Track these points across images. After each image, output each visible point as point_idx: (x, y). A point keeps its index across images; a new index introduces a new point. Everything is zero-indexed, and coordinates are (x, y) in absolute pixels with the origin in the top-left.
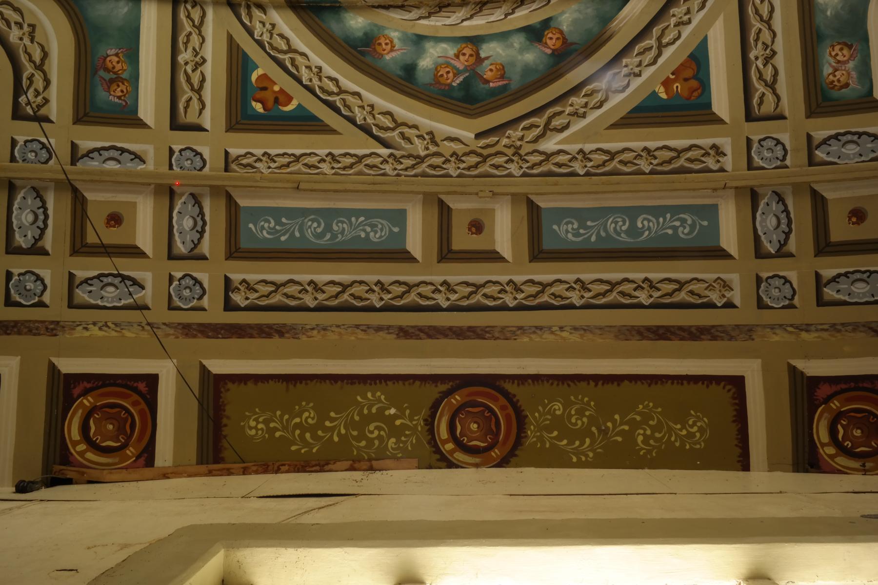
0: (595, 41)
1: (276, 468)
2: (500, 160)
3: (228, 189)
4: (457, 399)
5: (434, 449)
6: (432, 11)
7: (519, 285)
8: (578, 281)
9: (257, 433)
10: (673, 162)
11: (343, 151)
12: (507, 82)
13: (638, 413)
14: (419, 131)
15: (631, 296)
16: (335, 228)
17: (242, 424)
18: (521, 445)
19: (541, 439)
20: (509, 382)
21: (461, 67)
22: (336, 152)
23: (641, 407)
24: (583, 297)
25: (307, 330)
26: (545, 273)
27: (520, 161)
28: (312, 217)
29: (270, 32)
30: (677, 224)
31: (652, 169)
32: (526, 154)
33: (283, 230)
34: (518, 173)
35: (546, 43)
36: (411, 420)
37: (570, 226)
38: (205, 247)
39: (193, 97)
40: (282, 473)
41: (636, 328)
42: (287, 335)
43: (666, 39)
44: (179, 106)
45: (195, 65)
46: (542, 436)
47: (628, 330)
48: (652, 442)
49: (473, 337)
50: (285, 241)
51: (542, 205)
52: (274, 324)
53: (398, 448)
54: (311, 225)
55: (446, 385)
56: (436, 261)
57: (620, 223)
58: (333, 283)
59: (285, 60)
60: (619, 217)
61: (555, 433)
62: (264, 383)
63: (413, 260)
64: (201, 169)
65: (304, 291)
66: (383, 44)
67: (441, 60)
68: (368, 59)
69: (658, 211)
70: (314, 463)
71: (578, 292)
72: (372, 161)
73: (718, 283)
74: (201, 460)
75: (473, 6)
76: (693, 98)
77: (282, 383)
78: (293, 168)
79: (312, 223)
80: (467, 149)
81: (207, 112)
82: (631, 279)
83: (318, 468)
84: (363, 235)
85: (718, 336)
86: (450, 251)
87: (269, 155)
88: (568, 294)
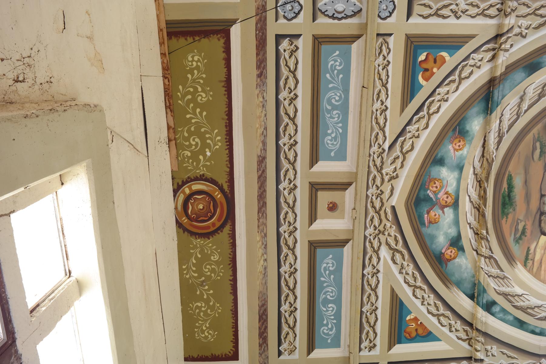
0: (446, 278)
1: (166, 76)
2: (376, 222)
3: (364, 36)
4: (218, 195)
5: (185, 181)
6: (478, 176)
7: (294, 234)
8: (296, 270)
9: (189, 61)
10: (368, 323)
11: (388, 117)
12: (427, 226)
13: (214, 304)
14: (399, 169)
15: (285, 301)
16: (335, 112)
17: (196, 51)
18: (191, 235)
19: (195, 247)
20: (231, 228)
21: (439, 196)
22: (388, 113)
23: (218, 305)
24: (286, 273)
25: (262, 93)
26: (302, 250)
27: (375, 234)
28: (343, 96)
29: (475, 65)
30: (330, 326)
31: (364, 312)
32: (379, 238)
33: (334, 75)
34: (367, 233)
35: (449, 249)
36: (203, 166)
37: (331, 265)
38: (322, 20)
40: (163, 80)
41: (266, 303)
42: (259, 80)
46: (197, 248)
47: (265, 299)
48: (197, 311)
49: (259, 205)
50: (326, 77)
51: (346, 248)
52: (266, 71)
53: (184, 158)
54: (337, 96)
55: (227, 188)
56: (311, 181)
57: (331, 295)
58: (296, 111)
59: (454, 76)
60: (335, 294)
61: (199, 256)
62: (225, 65)
63: (312, 166)
64: (379, 16)
65: (290, 91)
66: (459, 144)
67: (445, 182)
68: (450, 134)
69: (338, 315)
70: (171, 102)
71: (289, 270)
72: (380, 137)
73: (293, 348)
74: (168, 23)
75: (478, 203)
76: (405, 334)
77: (225, 78)
78: (378, 83)
79: (338, 96)
80: (385, 201)
81: (421, 20)
82: (296, 300)
83: (168, 104)
84: (329, 132)
85: (262, 347)
86: (317, 190)
87: (388, 65)
88: (287, 264)
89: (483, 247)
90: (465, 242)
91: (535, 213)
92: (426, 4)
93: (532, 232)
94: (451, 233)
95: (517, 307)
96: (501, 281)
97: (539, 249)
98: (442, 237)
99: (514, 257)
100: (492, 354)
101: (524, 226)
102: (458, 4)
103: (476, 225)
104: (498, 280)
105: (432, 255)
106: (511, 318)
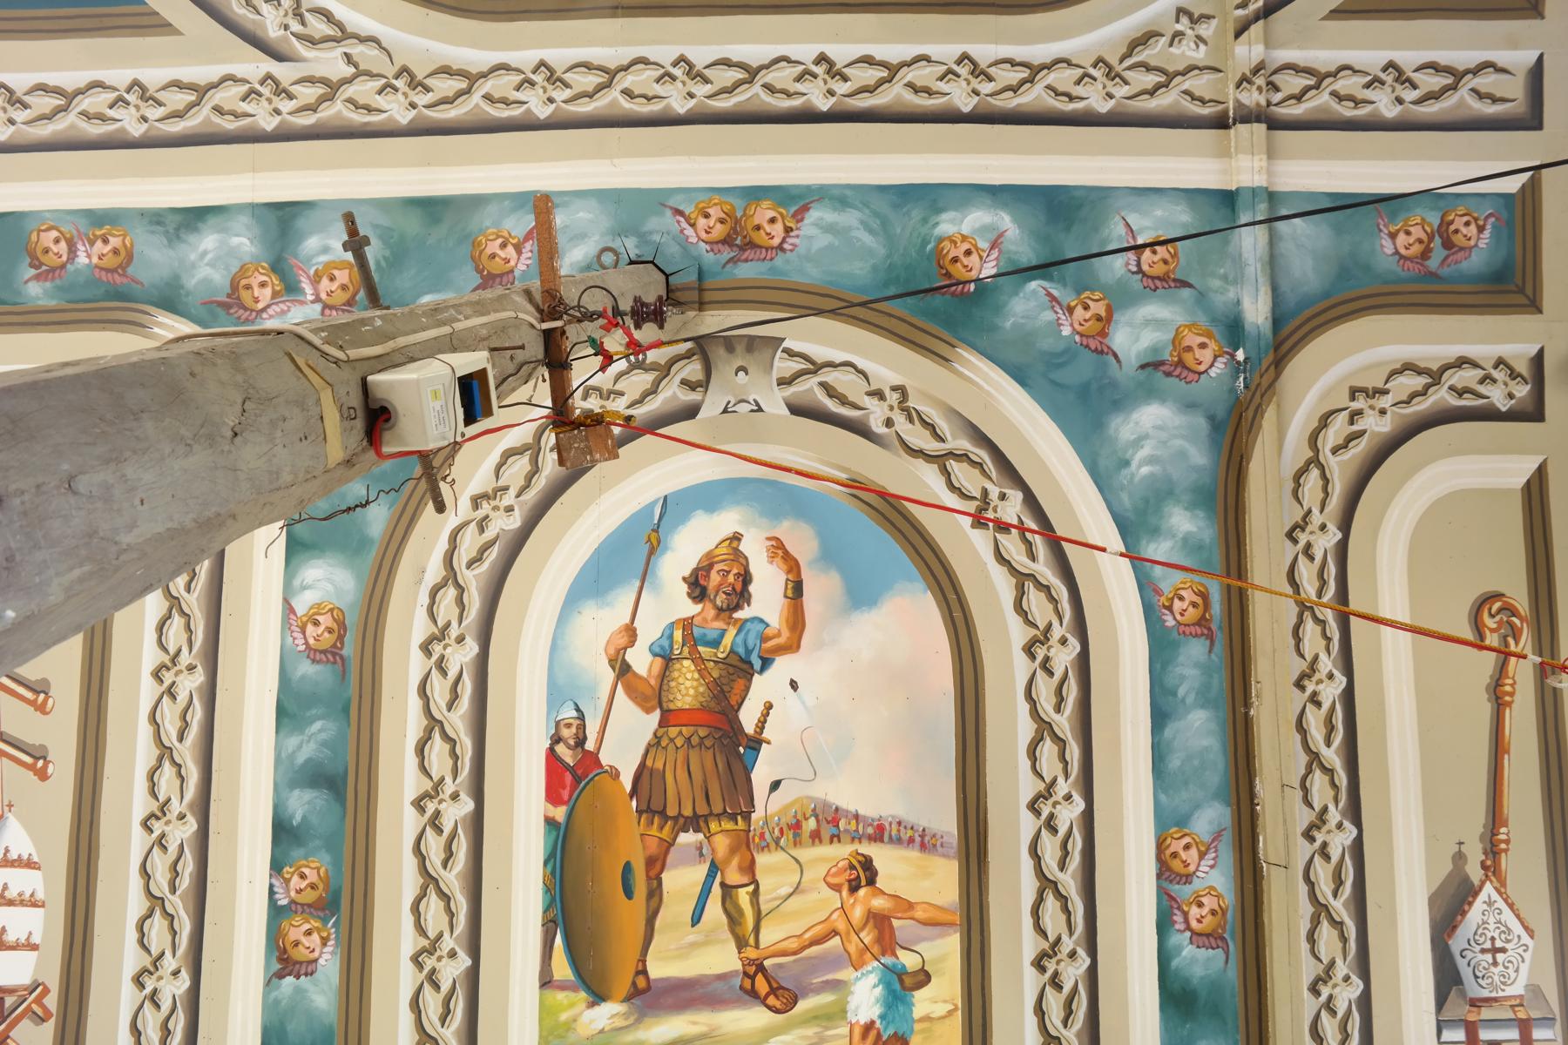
39: (1470, 86)
44: (1490, 114)
45: (1402, 84)
81: (1501, 57)
92: (1489, 101)
102: (1396, 103)
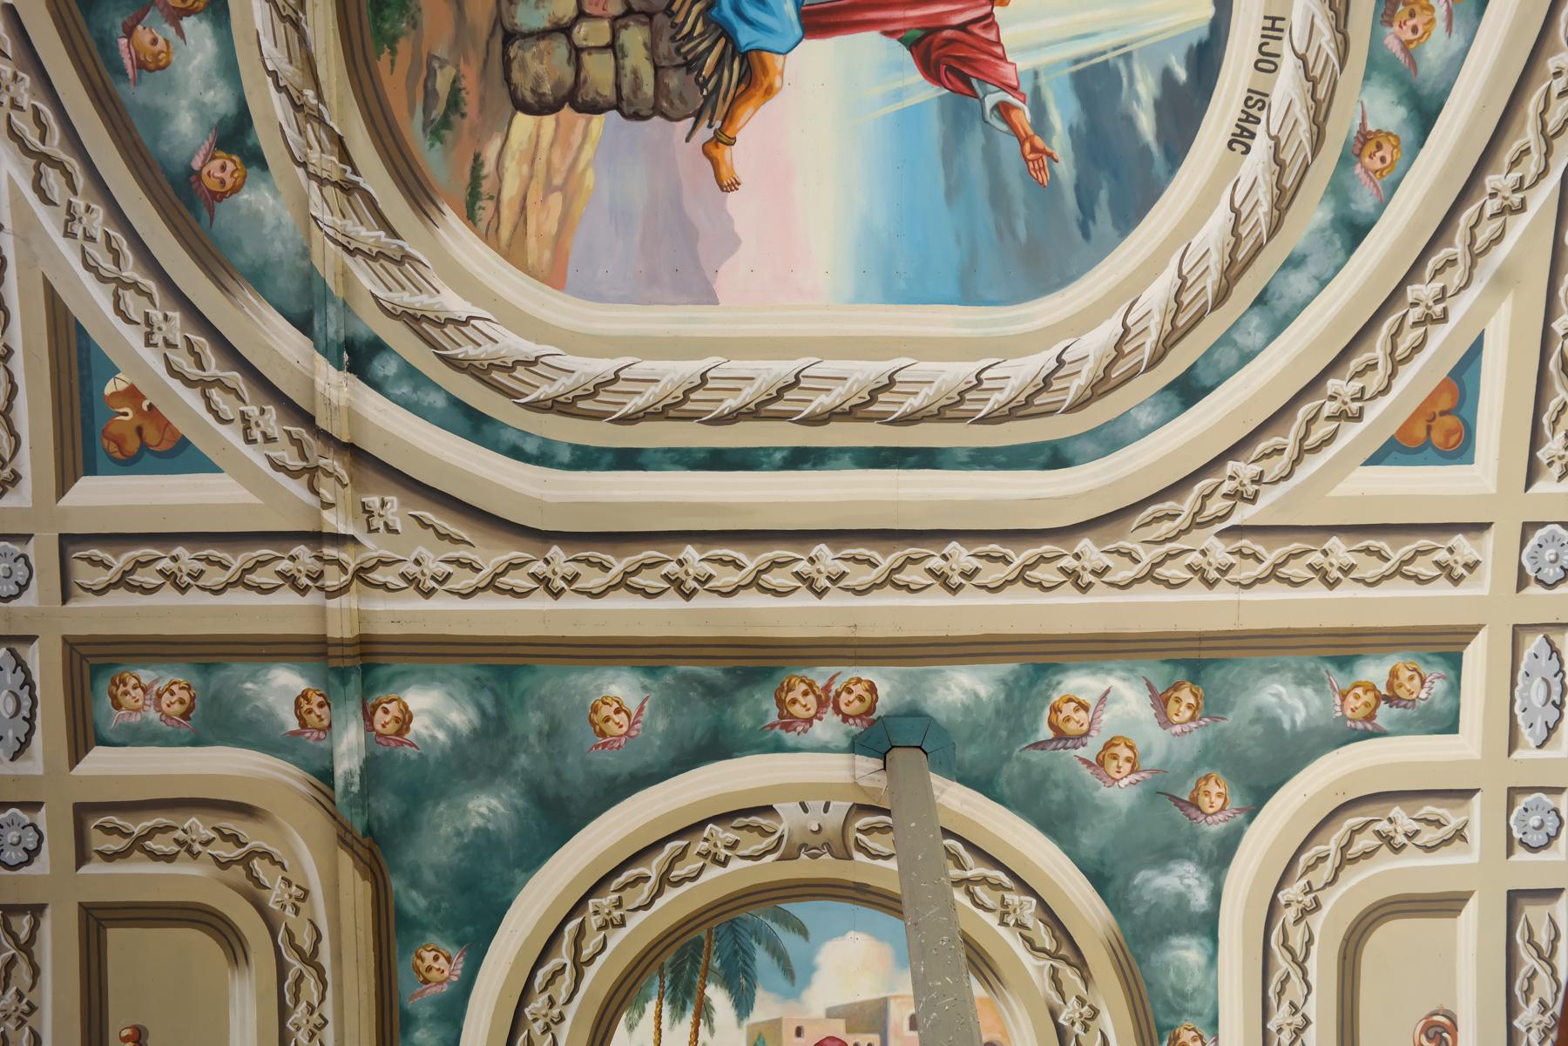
0: (213, 255)
12: (131, 75)
35: (214, 158)
43: (218, 396)
76: (106, 442)
89: (311, 148)
90: (264, 137)
91: (485, 36)
93: (482, 100)
94: (215, 105)
95: (456, 363)
96: (393, 269)
97: (513, 158)
98: (189, 120)
99: (430, 184)
100: (386, 524)
101: (454, 81)
103: (297, 78)
104: (382, 266)
105: (162, 178)
106: (439, 402)
